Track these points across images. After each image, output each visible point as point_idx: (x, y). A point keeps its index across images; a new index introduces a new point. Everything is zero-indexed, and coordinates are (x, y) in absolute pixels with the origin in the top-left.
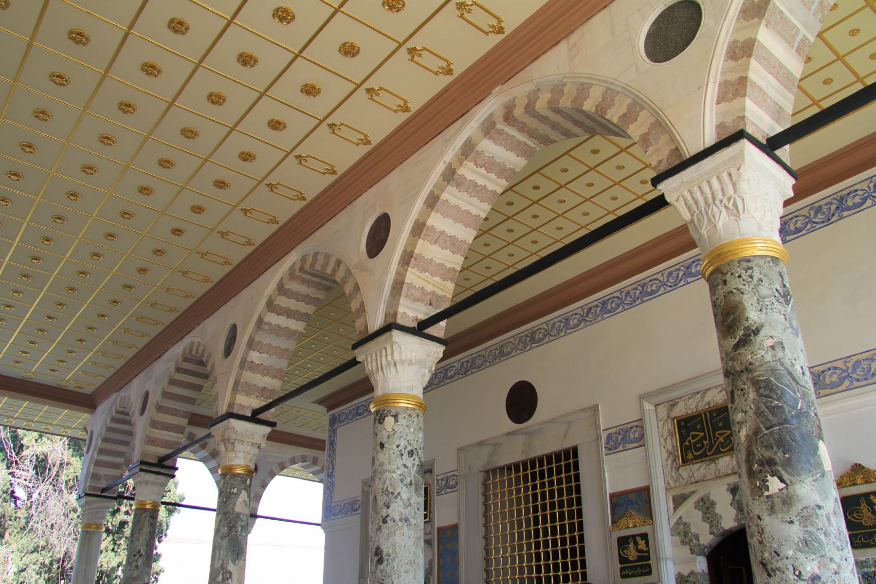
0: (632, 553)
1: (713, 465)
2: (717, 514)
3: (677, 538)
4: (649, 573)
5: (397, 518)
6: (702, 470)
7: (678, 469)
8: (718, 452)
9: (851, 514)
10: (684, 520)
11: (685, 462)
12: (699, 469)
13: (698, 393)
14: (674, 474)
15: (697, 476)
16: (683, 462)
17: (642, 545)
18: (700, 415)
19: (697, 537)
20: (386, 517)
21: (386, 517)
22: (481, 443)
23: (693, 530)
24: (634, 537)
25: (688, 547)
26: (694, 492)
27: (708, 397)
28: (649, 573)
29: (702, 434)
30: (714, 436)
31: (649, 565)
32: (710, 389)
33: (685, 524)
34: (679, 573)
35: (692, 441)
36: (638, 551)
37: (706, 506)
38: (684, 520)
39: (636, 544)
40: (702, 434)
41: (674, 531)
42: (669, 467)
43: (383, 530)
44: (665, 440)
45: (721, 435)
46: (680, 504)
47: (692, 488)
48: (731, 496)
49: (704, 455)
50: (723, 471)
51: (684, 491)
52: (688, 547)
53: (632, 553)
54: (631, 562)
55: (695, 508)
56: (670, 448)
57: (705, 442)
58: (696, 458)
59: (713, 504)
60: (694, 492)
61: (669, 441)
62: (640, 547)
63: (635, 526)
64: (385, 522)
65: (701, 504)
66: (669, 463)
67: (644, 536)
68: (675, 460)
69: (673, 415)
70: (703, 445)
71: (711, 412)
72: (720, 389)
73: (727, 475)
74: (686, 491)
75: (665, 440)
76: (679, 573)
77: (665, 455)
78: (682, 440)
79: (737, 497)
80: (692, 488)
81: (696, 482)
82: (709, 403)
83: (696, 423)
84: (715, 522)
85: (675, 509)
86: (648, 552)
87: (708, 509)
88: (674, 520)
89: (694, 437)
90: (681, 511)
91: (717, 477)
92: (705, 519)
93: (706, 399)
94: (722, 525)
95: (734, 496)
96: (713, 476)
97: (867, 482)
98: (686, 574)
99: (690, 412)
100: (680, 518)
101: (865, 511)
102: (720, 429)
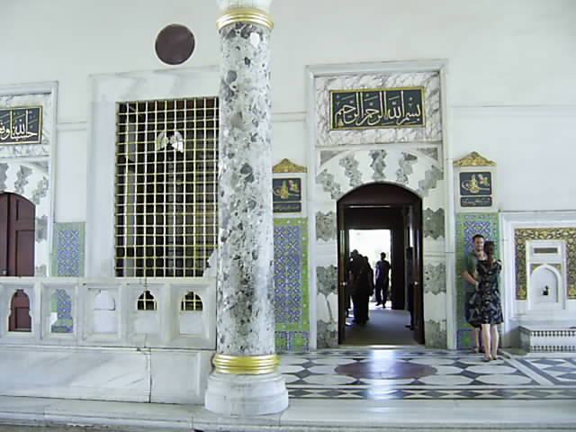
0: (284, 193)
1: (360, 134)
2: (358, 172)
3: (321, 185)
4: (299, 210)
5: (264, 138)
6: (350, 136)
7: (328, 132)
8: (365, 124)
9: (465, 184)
10: (328, 172)
11: (335, 127)
12: (345, 135)
13: (355, 75)
14: (324, 135)
15: (345, 140)
16: (334, 127)
17: (294, 186)
18: (355, 93)
19: (338, 187)
20: (256, 135)
21: (256, 135)
22: (120, 75)
23: (336, 180)
24: (287, 180)
25: (329, 193)
26: (340, 152)
27: (364, 80)
28: (299, 210)
29: (354, 108)
30: (364, 112)
31: (300, 204)
32: (365, 75)
33: (329, 175)
34: (319, 213)
35: (345, 112)
36: (290, 192)
37: (350, 164)
38: (328, 172)
39: (289, 186)
40: (354, 108)
41: (318, 180)
42: (321, 128)
43: (252, 147)
44: (320, 107)
45: (371, 112)
46: (327, 160)
47: (340, 149)
48: (372, 160)
49: (353, 125)
50: (368, 140)
51: (332, 149)
52: (329, 193)
53: (284, 193)
54: (282, 200)
55: (340, 164)
56: (323, 114)
57: (356, 115)
58: (346, 125)
59: (356, 163)
60: (340, 152)
61: (323, 107)
62: (292, 189)
63: (289, 171)
64: (253, 140)
65: (346, 162)
66: (321, 125)
67: (298, 181)
68: (326, 124)
69: (329, 88)
70: (354, 117)
71: (364, 93)
72: (374, 77)
73: (371, 144)
74: (334, 150)
75: (320, 107)
76: (319, 213)
77: (319, 120)
78: (335, 110)
79: (377, 161)
80: (340, 149)
81: (343, 145)
82: (363, 86)
83: (351, 99)
84: (356, 177)
85: (322, 163)
86: (300, 193)
87: (351, 166)
88: (320, 171)
89: (346, 109)
90: (328, 165)
91: (362, 144)
92: (348, 173)
93: (361, 82)
94: (362, 180)
95: (375, 159)
96: (359, 143)
97: (479, 165)
98: (325, 213)
99: (345, 89)
100: (325, 170)
101: (474, 183)
102: (371, 108)
